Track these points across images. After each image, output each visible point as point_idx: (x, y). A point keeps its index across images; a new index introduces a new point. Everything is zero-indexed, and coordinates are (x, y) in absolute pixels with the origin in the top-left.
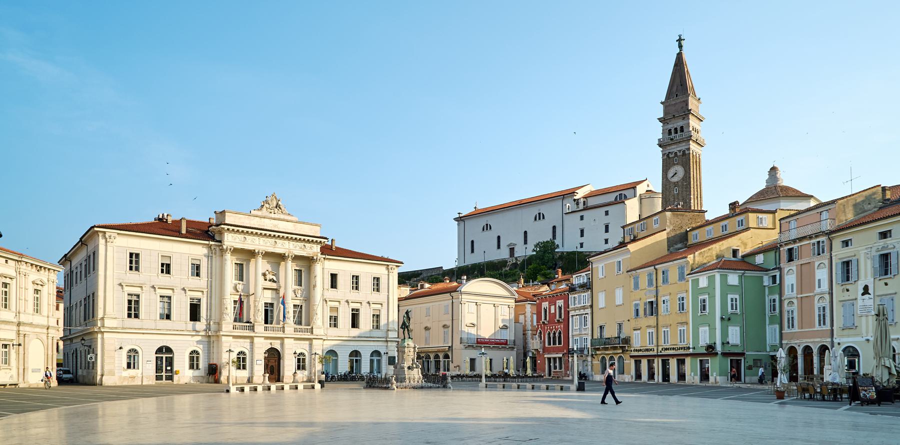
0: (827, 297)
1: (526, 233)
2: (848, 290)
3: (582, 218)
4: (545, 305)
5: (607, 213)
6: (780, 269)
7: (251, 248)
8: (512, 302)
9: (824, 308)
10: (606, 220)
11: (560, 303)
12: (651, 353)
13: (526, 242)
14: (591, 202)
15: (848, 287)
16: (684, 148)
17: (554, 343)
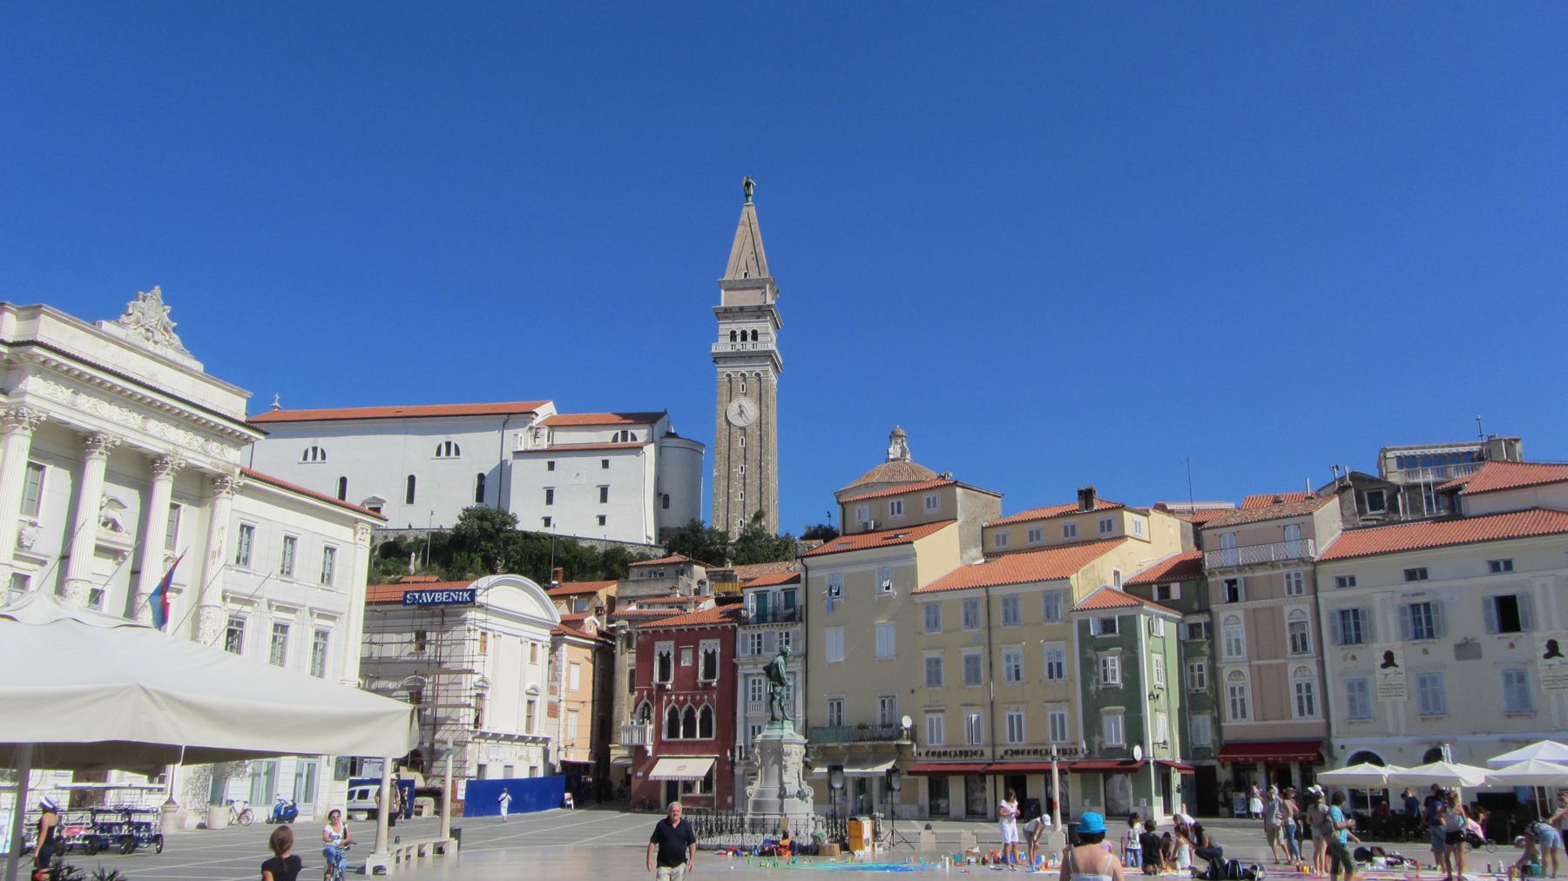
0: (1312, 666)
1: (412, 479)
2: (1354, 658)
3: (551, 466)
4: (664, 647)
5: (605, 464)
6: (1209, 611)
7: (85, 423)
8: (545, 636)
9: (1308, 686)
10: (604, 477)
11: (713, 645)
12: (976, 759)
13: (410, 499)
14: (563, 438)
15: (1353, 652)
16: (758, 370)
17: (690, 732)
